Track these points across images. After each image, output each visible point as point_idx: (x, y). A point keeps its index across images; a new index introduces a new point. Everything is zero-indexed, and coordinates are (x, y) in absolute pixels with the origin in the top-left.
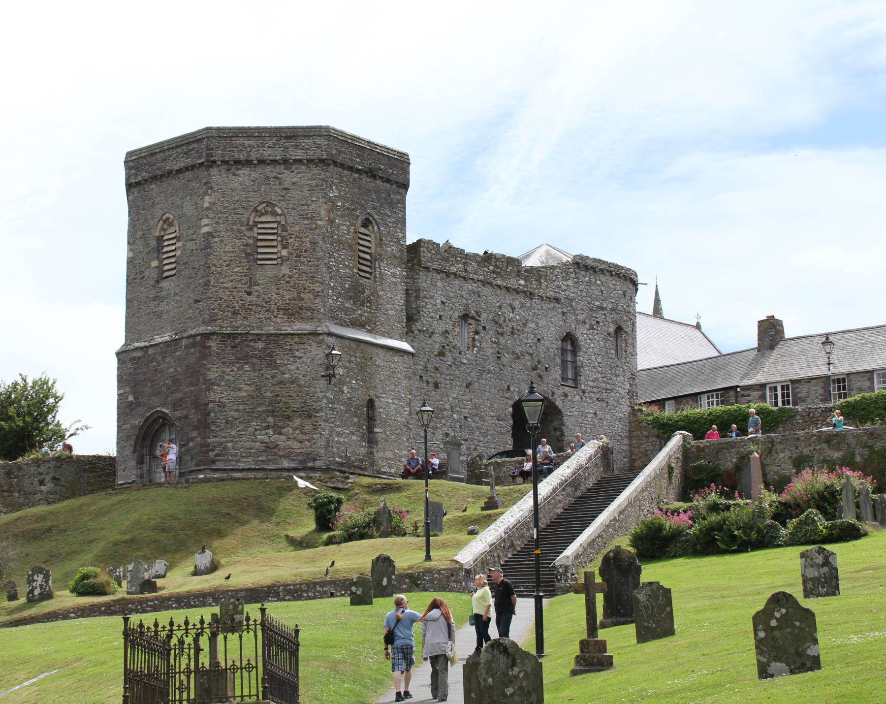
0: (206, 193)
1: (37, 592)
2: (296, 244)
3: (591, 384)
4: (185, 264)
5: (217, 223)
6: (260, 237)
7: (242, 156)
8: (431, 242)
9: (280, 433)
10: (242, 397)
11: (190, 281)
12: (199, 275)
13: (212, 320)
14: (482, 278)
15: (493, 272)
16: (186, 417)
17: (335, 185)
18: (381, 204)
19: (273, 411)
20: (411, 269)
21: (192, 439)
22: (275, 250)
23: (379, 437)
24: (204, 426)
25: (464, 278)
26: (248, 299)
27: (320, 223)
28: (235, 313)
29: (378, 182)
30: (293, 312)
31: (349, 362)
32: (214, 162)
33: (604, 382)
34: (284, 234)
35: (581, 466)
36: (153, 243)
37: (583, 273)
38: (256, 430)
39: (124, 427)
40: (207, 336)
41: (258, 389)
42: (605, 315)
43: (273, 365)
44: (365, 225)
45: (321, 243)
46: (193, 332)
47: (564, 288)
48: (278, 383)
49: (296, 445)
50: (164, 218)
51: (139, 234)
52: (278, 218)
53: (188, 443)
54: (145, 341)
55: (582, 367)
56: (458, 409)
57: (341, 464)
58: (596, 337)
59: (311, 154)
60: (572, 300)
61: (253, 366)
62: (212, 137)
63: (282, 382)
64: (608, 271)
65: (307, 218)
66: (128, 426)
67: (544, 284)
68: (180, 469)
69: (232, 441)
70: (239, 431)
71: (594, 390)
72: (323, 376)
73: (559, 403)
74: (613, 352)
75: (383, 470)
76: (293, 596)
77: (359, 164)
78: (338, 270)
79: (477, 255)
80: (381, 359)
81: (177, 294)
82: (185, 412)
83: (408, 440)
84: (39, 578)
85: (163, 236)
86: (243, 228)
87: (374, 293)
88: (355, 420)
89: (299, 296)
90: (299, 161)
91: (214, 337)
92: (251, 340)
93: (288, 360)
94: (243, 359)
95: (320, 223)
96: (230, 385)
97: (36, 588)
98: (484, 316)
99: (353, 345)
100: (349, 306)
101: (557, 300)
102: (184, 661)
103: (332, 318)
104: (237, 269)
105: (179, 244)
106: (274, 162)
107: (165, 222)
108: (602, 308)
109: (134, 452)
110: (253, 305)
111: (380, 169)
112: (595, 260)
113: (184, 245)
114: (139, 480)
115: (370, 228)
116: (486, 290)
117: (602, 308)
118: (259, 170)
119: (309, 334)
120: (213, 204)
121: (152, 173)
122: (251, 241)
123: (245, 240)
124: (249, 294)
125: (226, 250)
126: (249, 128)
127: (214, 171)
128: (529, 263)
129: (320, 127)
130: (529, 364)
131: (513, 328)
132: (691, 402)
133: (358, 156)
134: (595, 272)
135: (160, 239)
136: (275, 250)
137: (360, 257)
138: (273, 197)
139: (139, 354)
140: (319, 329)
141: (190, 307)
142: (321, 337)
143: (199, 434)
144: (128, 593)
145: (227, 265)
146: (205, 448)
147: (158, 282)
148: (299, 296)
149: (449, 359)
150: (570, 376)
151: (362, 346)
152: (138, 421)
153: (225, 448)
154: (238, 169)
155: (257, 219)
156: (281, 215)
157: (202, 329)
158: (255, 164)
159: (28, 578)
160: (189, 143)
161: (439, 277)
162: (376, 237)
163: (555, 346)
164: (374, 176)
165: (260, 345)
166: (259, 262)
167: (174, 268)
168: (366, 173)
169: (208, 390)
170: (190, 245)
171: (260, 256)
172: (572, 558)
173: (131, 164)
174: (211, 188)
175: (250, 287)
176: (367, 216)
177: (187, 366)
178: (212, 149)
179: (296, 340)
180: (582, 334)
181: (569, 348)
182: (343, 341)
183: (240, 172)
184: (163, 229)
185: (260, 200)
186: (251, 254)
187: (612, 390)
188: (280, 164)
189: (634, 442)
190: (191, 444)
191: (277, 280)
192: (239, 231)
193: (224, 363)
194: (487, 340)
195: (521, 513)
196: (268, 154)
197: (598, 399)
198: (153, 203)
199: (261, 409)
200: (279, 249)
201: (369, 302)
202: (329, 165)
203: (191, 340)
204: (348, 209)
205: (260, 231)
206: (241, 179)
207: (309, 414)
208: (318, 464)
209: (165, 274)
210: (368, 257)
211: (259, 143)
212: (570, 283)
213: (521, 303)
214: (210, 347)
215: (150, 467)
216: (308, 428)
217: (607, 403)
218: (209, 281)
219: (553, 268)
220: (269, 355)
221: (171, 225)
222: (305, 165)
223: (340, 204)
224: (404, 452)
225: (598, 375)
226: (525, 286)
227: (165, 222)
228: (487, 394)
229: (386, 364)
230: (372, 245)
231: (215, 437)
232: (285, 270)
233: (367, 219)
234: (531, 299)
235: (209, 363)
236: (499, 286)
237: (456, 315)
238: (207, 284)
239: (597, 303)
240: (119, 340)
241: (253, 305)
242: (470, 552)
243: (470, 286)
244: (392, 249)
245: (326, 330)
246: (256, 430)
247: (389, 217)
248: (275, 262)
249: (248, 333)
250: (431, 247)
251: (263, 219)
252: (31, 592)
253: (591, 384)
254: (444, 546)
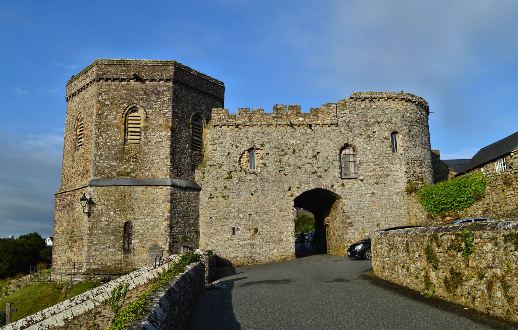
3: (370, 173)
56: (244, 210)
58: (373, 142)
71: (372, 177)
77: (124, 75)
100: (115, 164)
149: (235, 179)
189: (410, 207)
197: (376, 183)
201: (136, 158)
239: (373, 120)
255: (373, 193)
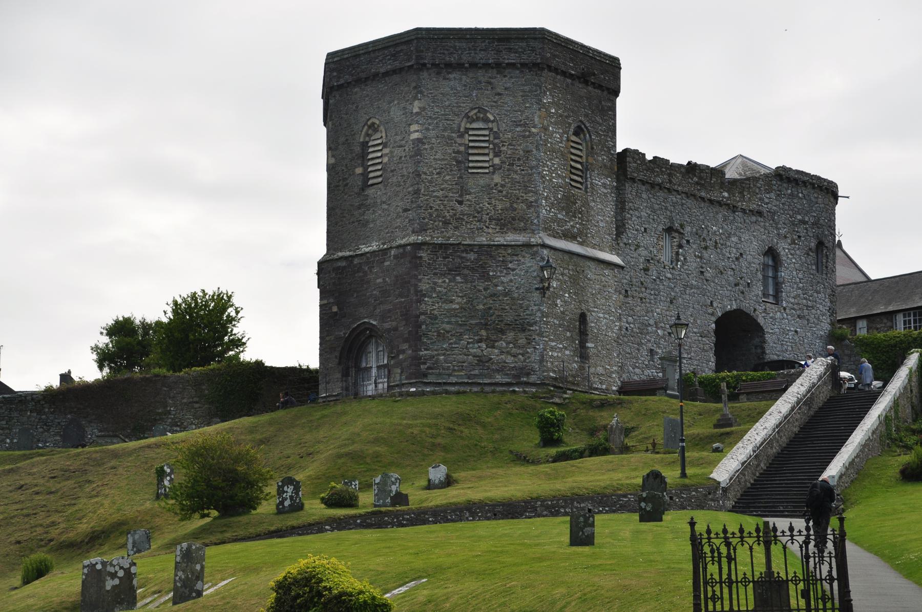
0: (415, 98)
1: (287, 503)
2: (509, 152)
3: (793, 300)
4: (392, 171)
5: (427, 129)
6: (471, 144)
7: (453, 59)
8: (636, 152)
9: (493, 347)
10: (455, 309)
11: (398, 189)
12: (409, 183)
13: (423, 230)
14: (686, 189)
15: (697, 183)
16: (396, 329)
17: (549, 90)
18: (593, 112)
19: (486, 324)
20: (618, 180)
21: (403, 352)
22: (487, 158)
23: (592, 352)
24: (416, 338)
25: (668, 189)
26: (459, 208)
27: (533, 130)
28: (446, 223)
29: (590, 88)
30: (505, 223)
31: (562, 274)
32: (424, 65)
33: (805, 299)
34: (496, 141)
35: (814, 385)
36: (358, 149)
37: (785, 185)
38: (468, 343)
39: (328, 338)
40: (417, 246)
41: (470, 301)
42: (806, 229)
43: (485, 277)
44: (576, 133)
45: (535, 152)
46: (403, 242)
47: (767, 200)
48: (491, 296)
49: (510, 359)
50: (369, 123)
51: (342, 139)
52: (490, 125)
53: (398, 355)
54: (350, 251)
55: (783, 283)
57: (555, 379)
58: (798, 252)
59: (525, 58)
60: (774, 213)
61: (465, 277)
62: (422, 38)
63: (495, 295)
64: (811, 184)
65: (520, 125)
66: (332, 338)
67: (747, 196)
68: (388, 382)
69: (444, 354)
70: (451, 344)
71: (795, 307)
72: (537, 289)
73: (761, 321)
74: (814, 267)
75: (595, 386)
76: (551, 512)
77: (572, 68)
78: (551, 180)
79: (682, 166)
80: (592, 272)
81: (384, 202)
82: (394, 324)
83: (618, 356)
84: (290, 490)
85: (367, 142)
86: (453, 135)
87: (586, 204)
88: (568, 334)
89: (511, 206)
90: (512, 65)
91: (425, 247)
92: (463, 252)
93: (501, 272)
94: (454, 271)
95: (533, 130)
96: (442, 297)
97: (286, 499)
98: (688, 229)
99: (566, 257)
101: (760, 213)
102: (825, 568)
103: (546, 229)
104: (447, 178)
105: (386, 151)
106: (487, 66)
107: (370, 127)
108: (805, 223)
109: (339, 363)
110: (464, 215)
111: (594, 74)
112: (798, 172)
113: (391, 152)
114: (345, 392)
115: (582, 136)
116: (690, 202)
117: (803, 222)
118: (471, 75)
119: (523, 245)
120: (423, 109)
121: (355, 78)
122: (462, 149)
123: (456, 147)
124: (460, 203)
125: (437, 157)
126: (460, 30)
127: (425, 74)
128: (730, 174)
129: (534, 30)
130: (731, 279)
131: (716, 242)
132: (885, 321)
133: (572, 60)
134: (797, 184)
135: (365, 145)
136: (487, 158)
137: (572, 167)
138: (485, 103)
139: (344, 264)
140: (532, 240)
141: (398, 216)
142: (535, 249)
143: (410, 347)
144: (375, 506)
145: (438, 173)
146: (417, 360)
147: (363, 190)
148: (511, 206)
149: (654, 274)
150: (771, 292)
151: (575, 259)
152: (343, 333)
153: (437, 361)
154: (450, 73)
155: (468, 126)
156: (493, 122)
157: (412, 239)
158: (466, 68)
159: (278, 490)
160: (397, 45)
161: (644, 188)
162: (587, 146)
163: (757, 261)
164: (586, 82)
165: (472, 256)
166: (470, 171)
167: (381, 176)
168: (579, 78)
169: (419, 301)
170: (398, 152)
171: (471, 165)
172: (837, 478)
173: (332, 66)
174: (421, 92)
175: (461, 196)
176: (579, 124)
177: (396, 277)
178: (422, 51)
179: (509, 251)
180: (783, 248)
181: (770, 263)
182: (556, 253)
183: (451, 76)
184: (368, 135)
185: (471, 105)
186: (461, 162)
187: (813, 307)
188: (492, 68)
190: (401, 357)
191: (488, 189)
192: (450, 138)
193: (435, 274)
194: (691, 252)
195: (766, 431)
196: (480, 57)
197: (799, 317)
198: (357, 107)
199: (473, 322)
200: (491, 156)
201: (580, 213)
202: (543, 69)
203: (401, 250)
204: (561, 116)
205: (471, 138)
206: (452, 83)
207: (523, 326)
208: (533, 378)
209: (370, 182)
210: (579, 166)
211: (471, 45)
212: (773, 195)
213: (724, 216)
214: (421, 257)
215: (356, 380)
216: (522, 341)
217: (808, 320)
218: (419, 190)
219: (755, 179)
220: (482, 267)
221: (376, 130)
222: (518, 69)
223: (553, 111)
224: (615, 368)
225: (800, 292)
226: (728, 199)
227: (370, 127)
228: (691, 309)
229: (597, 277)
230: (583, 154)
231: (426, 350)
232: (497, 179)
233: (579, 127)
234: (734, 212)
235: (420, 274)
236: (703, 199)
237: (660, 228)
238: (417, 192)
239: (799, 217)
240: (320, 249)
241: (464, 215)
242: (725, 470)
243: (673, 198)
244: (603, 158)
245: (540, 241)
246: (468, 343)
247: (600, 125)
248: (487, 171)
249: (460, 244)
250: (637, 157)
251: (475, 125)
252: (282, 503)
253: (793, 300)
254: (698, 463)
255: (796, 332)
